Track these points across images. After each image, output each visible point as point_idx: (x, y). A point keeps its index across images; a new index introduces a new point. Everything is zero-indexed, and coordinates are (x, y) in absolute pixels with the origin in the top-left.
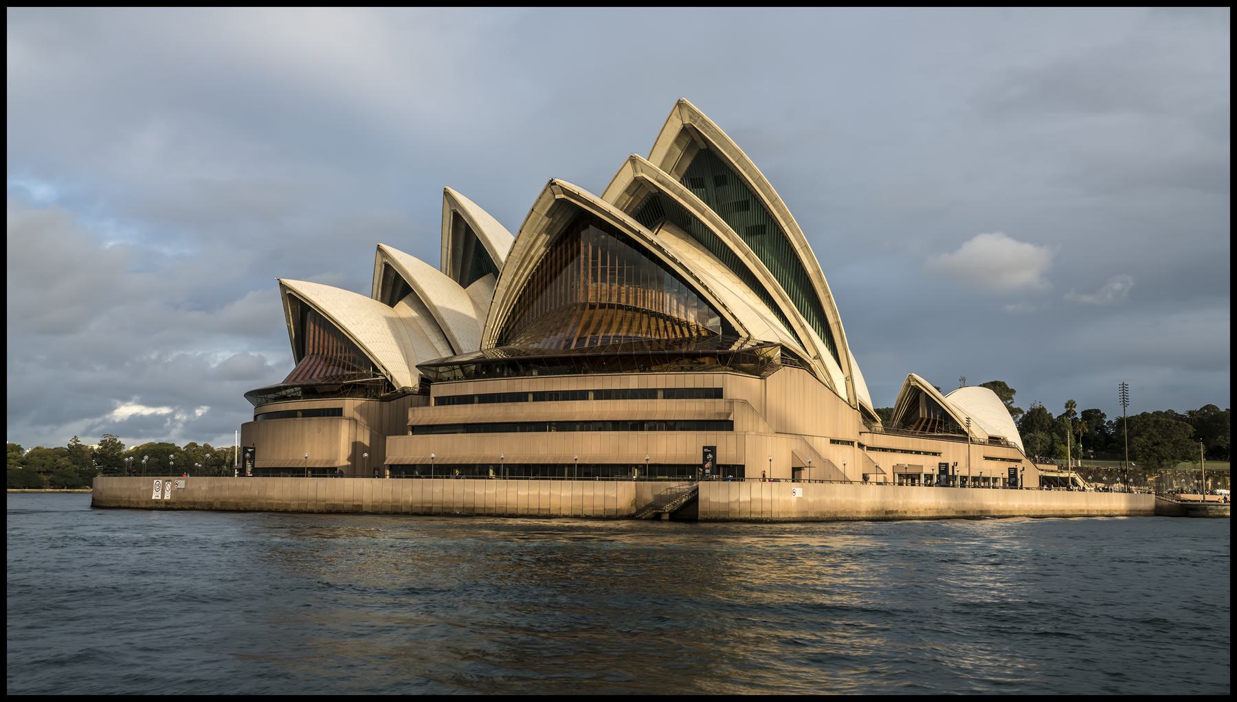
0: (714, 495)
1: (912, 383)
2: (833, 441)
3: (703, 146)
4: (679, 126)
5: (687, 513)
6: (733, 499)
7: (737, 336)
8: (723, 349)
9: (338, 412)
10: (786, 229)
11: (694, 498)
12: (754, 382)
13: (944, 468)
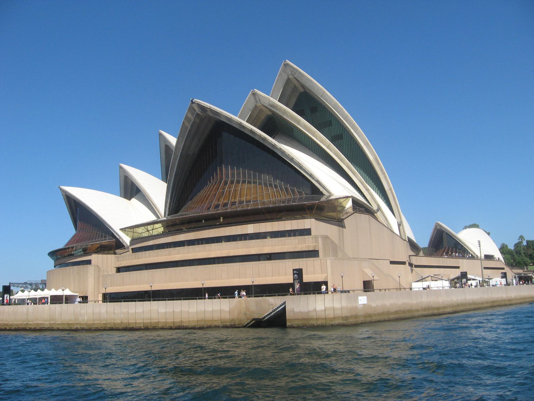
0: (298, 306)
1: (438, 227)
2: (392, 263)
3: (301, 90)
5: (278, 320)
6: (311, 308)
7: (322, 194)
8: (314, 204)
9: (89, 262)
10: (355, 134)
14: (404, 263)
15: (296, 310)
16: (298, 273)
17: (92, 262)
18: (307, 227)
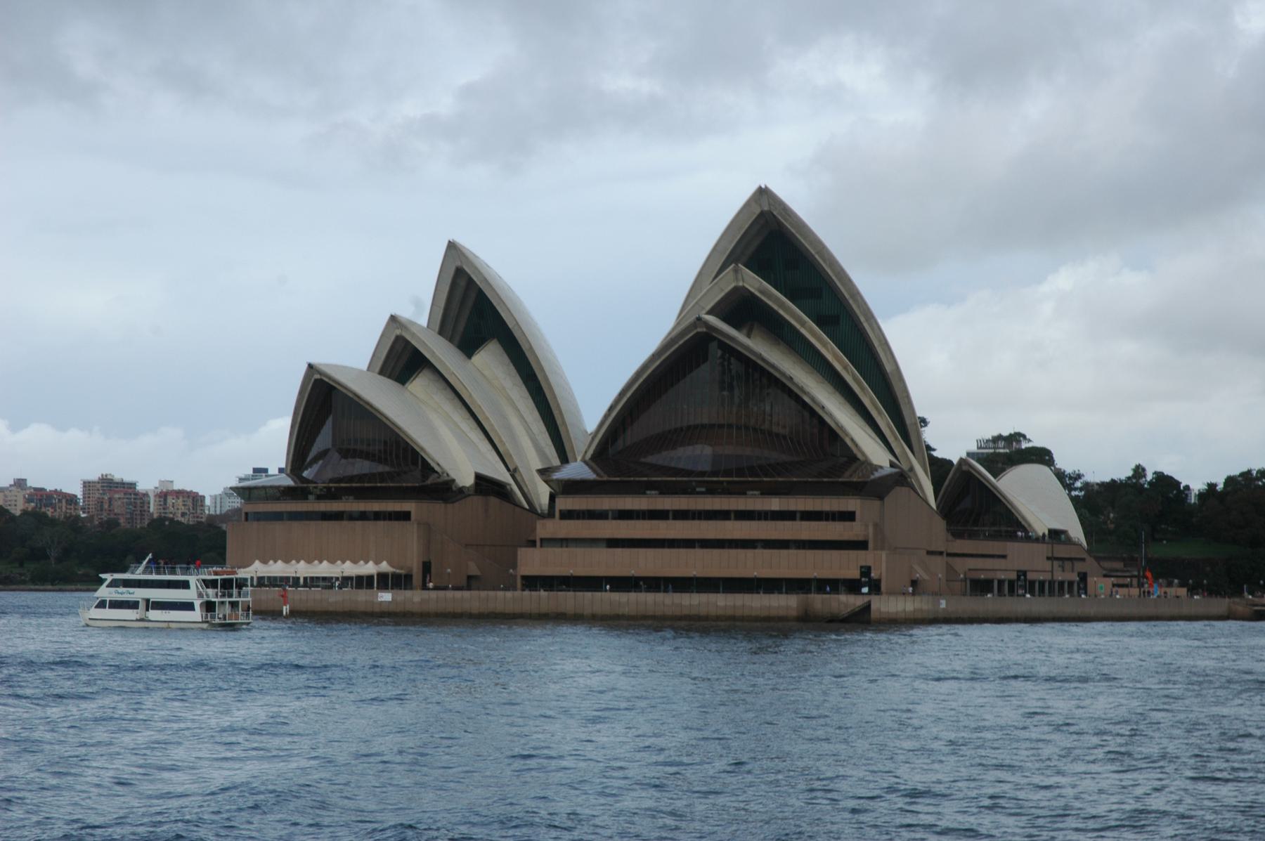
1: (965, 468)
2: (929, 553)
4: (758, 211)
9: (405, 516)
11: (867, 608)
12: (877, 503)
16: (866, 571)
17: (413, 516)
18: (851, 509)
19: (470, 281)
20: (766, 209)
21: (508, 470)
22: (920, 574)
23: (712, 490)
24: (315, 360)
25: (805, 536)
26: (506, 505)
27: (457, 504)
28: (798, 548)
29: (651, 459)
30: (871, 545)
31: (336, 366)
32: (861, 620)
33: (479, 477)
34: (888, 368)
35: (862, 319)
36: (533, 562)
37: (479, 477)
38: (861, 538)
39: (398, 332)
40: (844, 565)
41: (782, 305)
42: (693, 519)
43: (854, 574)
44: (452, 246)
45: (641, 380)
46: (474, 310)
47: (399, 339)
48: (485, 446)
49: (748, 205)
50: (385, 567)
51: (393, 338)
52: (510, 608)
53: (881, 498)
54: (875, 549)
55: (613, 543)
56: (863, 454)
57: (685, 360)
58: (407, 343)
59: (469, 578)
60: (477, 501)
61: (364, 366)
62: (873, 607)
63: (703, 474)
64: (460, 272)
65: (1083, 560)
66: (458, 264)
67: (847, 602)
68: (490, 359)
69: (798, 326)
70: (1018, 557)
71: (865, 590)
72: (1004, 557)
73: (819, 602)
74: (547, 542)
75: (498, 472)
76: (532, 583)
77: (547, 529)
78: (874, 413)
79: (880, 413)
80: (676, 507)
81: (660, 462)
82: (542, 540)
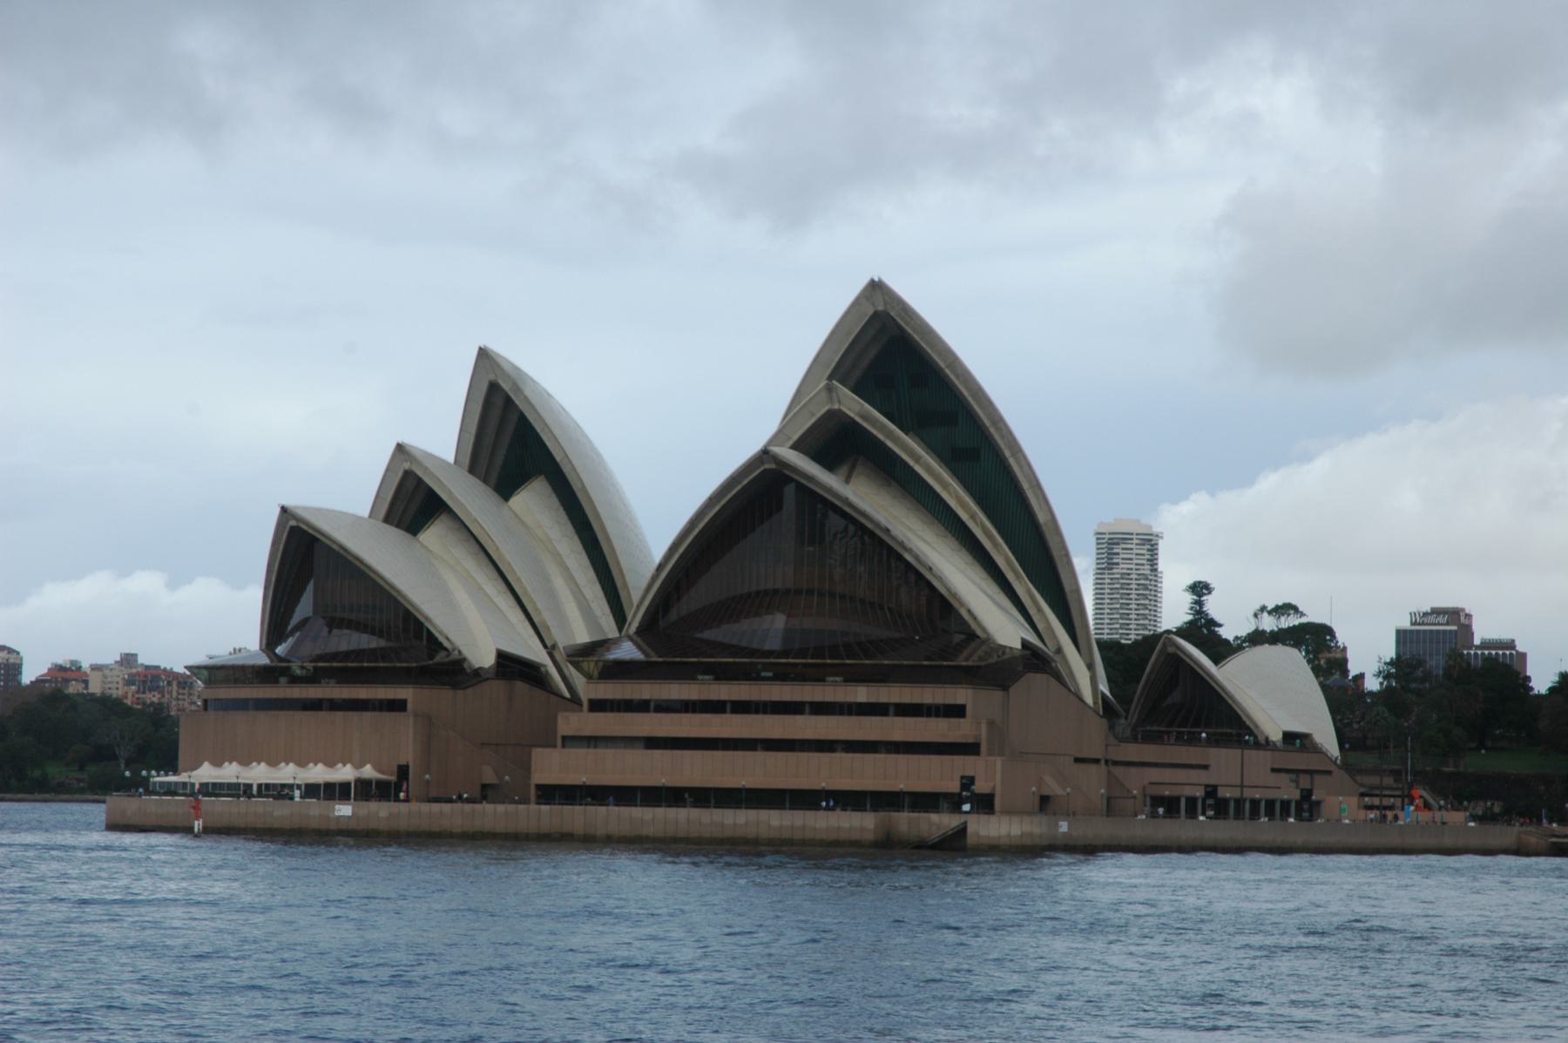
1: (1171, 650)
2: (1077, 760)
4: (871, 312)
9: (398, 706)
11: (962, 831)
12: (997, 695)
13: (1211, 791)
14: (1097, 761)
15: (983, 833)
16: (968, 782)
17: (410, 706)
19: (509, 402)
20: (881, 308)
21: (545, 646)
22: (1053, 787)
23: (782, 676)
24: (290, 502)
25: (809, 734)
26: (538, 693)
27: (469, 691)
28: (889, 752)
29: (708, 635)
30: (983, 749)
31: (319, 510)
32: (954, 846)
33: (502, 656)
34: (1041, 517)
35: (1007, 453)
36: (552, 766)
37: (502, 656)
38: (971, 740)
39: (407, 466)
40: (939, 775)
41: (890, 435)
42: (757, 712)
43: (954, 786)
44: (483, 354)
45: (696, 531)
46: (512, 439)
47: (408, 474)
48: (516, 615)
49: (856, 303)
50: (368, 772)
51: (400, 474)
52: (501, 827)
53: (1005, 688)
54: (990, 754)
55: (652, 743)
56: (984, 630)
57: (755, 503)
58: (420, 481)
59: (484, 787)
60: (498, 688)
61: (364, 510)
62: (971, 829)
63: (770, 654)
64: (494, 388)
65: (1329, 773)
66: (492, 377)
67: (941, 822)
68: (533, 502)
69: (911, 463)
70: (1224, 767)
71: (966, 807)
72: (1206, 767)
73: (906, 822)
74: (568, 741)
75: (533, 651)
76: (550, 794)
77: (572, 723)
78: (1010, 577)
79: (1018, 577)
80: (734, 697)
81: (720, 639)
82: (564, 738)
